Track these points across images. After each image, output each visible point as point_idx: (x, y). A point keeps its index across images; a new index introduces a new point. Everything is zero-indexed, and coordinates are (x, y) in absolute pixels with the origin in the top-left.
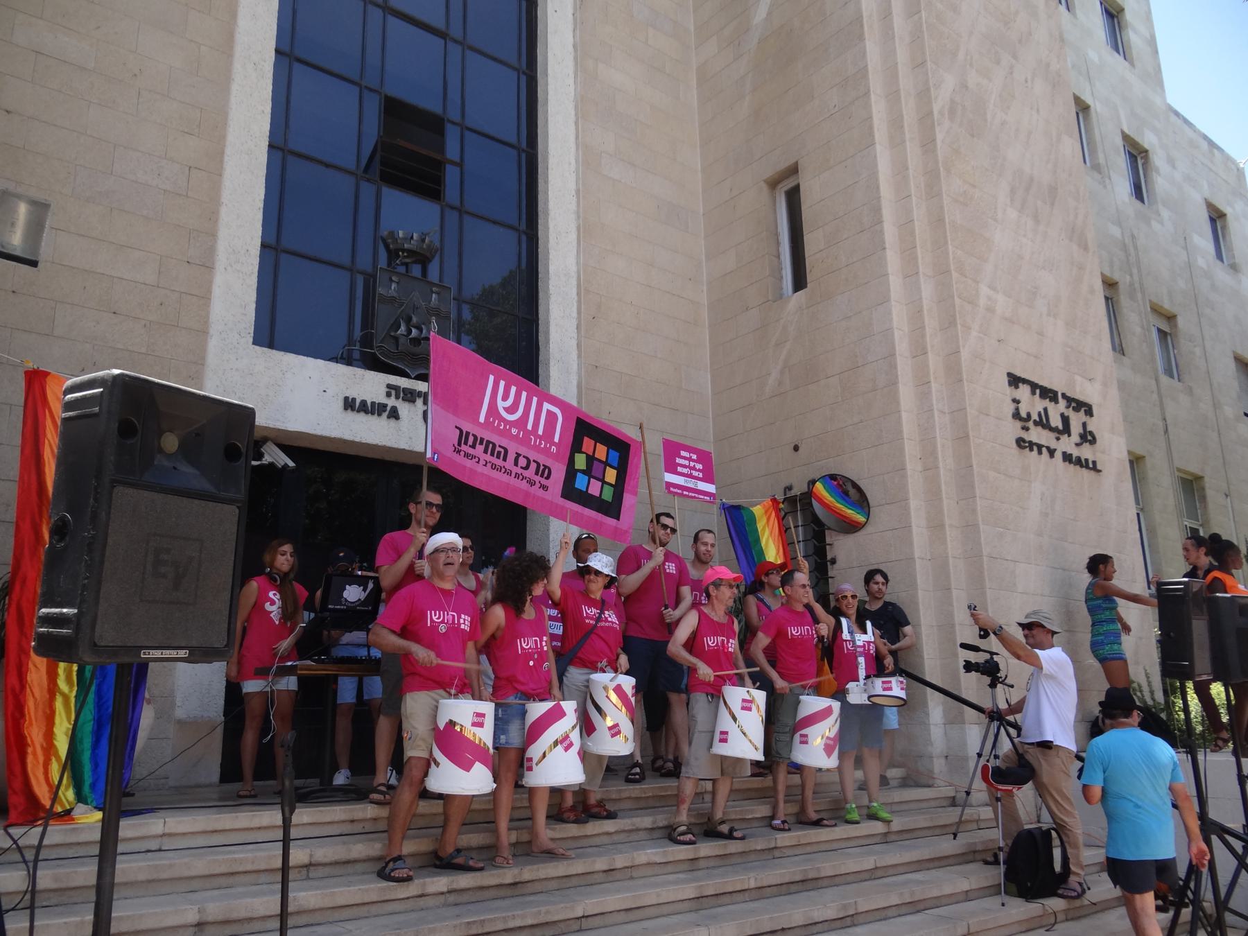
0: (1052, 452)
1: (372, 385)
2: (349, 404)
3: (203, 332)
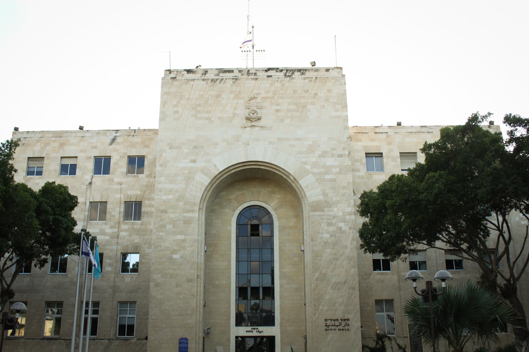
0: (335, 330)
1: (249, 328)
2: (247, 331)
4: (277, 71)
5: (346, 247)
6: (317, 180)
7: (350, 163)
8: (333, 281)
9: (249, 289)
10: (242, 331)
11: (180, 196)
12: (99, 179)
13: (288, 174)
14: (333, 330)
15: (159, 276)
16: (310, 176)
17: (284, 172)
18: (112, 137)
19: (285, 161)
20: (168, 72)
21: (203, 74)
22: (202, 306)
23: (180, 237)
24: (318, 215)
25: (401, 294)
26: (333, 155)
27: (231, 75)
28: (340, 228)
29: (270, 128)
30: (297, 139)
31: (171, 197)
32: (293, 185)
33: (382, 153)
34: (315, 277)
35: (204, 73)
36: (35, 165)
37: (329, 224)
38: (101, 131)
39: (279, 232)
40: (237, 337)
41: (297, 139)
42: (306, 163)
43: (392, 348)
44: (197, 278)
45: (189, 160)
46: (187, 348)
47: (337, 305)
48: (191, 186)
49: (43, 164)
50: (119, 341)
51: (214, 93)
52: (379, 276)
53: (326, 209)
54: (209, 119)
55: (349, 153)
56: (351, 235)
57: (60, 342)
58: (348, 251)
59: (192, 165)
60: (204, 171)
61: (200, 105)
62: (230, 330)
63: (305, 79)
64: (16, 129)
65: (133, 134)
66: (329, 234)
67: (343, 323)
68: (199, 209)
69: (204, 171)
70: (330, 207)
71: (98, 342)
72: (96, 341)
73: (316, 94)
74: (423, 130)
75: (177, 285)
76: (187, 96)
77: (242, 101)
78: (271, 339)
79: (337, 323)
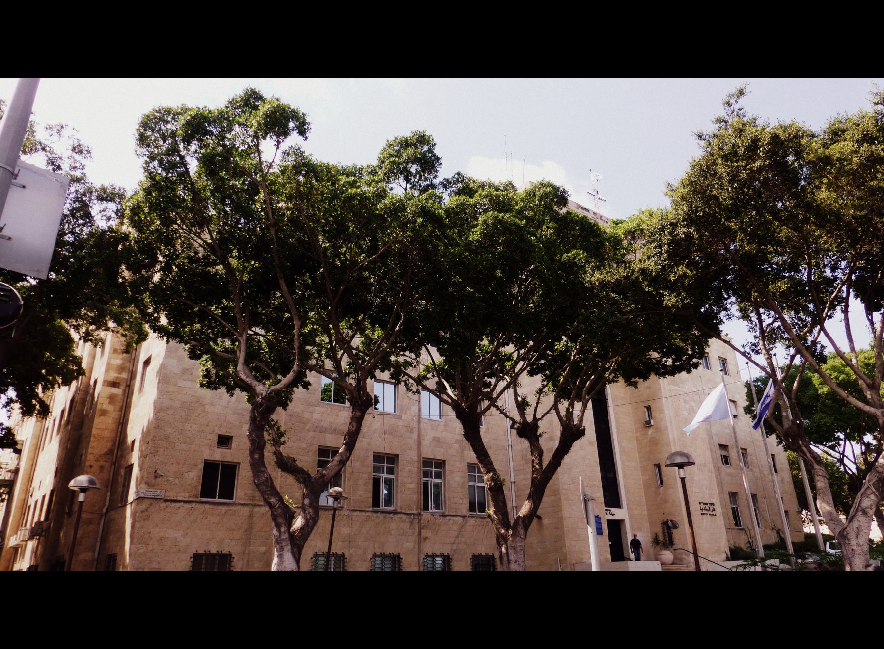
72: (448, 518)
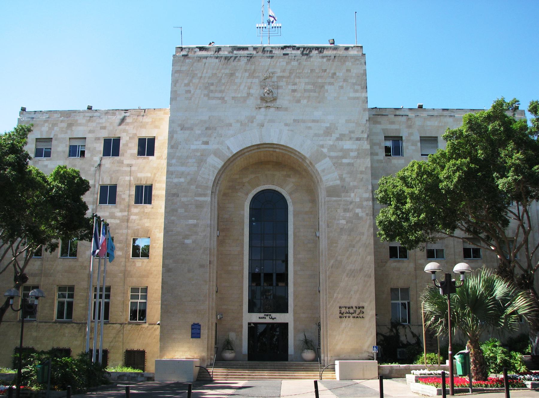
1: (262, 315)
2: (259, 318)
3: (242, 313)
4: (293, 49)
5: (363, 234)
6: (334, 164)
7: (368, 147)
8: (348, 268)
9: (262, 275)
10: (255, 318)
11: (191, 179)
12: (108, 161)
13: (304, 158)
14: (347, 318)
15: (171, 261)
16: (327, 159)
17: (299, 155)
18: (121, 117)
19: (301, 143)
20: (180, 50)
21: (216, 52)
22: (215, 292)
23: (191, 222)
24: (334, 201)
25: (417, 282)
26: (351, 139)
27: (246, 52)
28: (358, 214)
29: (286, 109)
30: (314, 121)
31: (182, 180)
32: (309, 169)
33: (402, 137)
34: (331, 264)
35: (217, 50)
36: (42, 146)
37: (345, 210)
38: (109, 110)
39: (294, 217)
40: (249, 324)
41: (314, 121)
42: (322, 146)
43: (406, 336)
44: (210, 264)
45: (201, 142)
46: (200, 334)
47: (352, 293)
48: (203, 169)
49: (51, 145)
50: (131, 325)
51: (227, 71)
52: (395, 264)
53: (343, 194)
54: (222, 99)
55: (368, 136)
56: (368, 222)
57: (73, 326)
58: (364, 238)
59: (204, 147)
60: (216, 153)
61: (212, 84)
62: (242, 317)
63: (323, 57)
64: (23, 109)
65: (142, 113)
66: (345, 221)
67: (358, 311)
68: (212, 192)
69: (216, 153)
70: (347, 192)
71: (110, 327)
73: (334, 74)
74: (445, 113)
75: (189, 271)
76: (199, 75)
77: (256, 81)
78: (285, 326)
79: (351, 311)
